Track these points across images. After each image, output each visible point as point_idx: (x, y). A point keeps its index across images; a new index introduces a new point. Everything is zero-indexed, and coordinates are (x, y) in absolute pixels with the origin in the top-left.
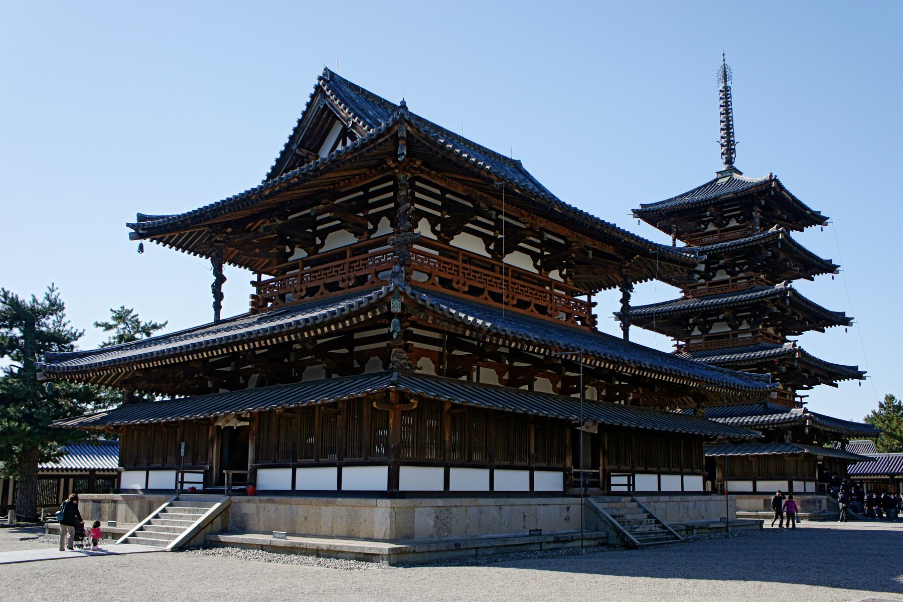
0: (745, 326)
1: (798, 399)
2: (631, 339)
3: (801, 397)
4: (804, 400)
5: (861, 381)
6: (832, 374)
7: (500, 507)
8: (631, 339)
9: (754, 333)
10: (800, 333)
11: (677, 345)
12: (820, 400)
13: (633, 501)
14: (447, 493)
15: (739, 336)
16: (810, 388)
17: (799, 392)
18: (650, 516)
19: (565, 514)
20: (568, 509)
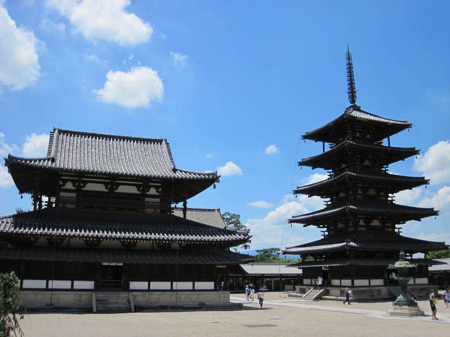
0: (351, 193)
1: (396, 230)
2: (187, 218)
3: (399, 229)
4: (400, 230)
5: (436, 216)
6: (418, 214)
7: (36, 295)
8: (187, 218)
10: (397, 191)
11: (327, 205)
12: (409, 229)
13: (128, 294)
15: (350, 198)
16: (404, 223)
17: (397, 226)
18: (129, 301)
19: (78, 298)
20: (80, 296)
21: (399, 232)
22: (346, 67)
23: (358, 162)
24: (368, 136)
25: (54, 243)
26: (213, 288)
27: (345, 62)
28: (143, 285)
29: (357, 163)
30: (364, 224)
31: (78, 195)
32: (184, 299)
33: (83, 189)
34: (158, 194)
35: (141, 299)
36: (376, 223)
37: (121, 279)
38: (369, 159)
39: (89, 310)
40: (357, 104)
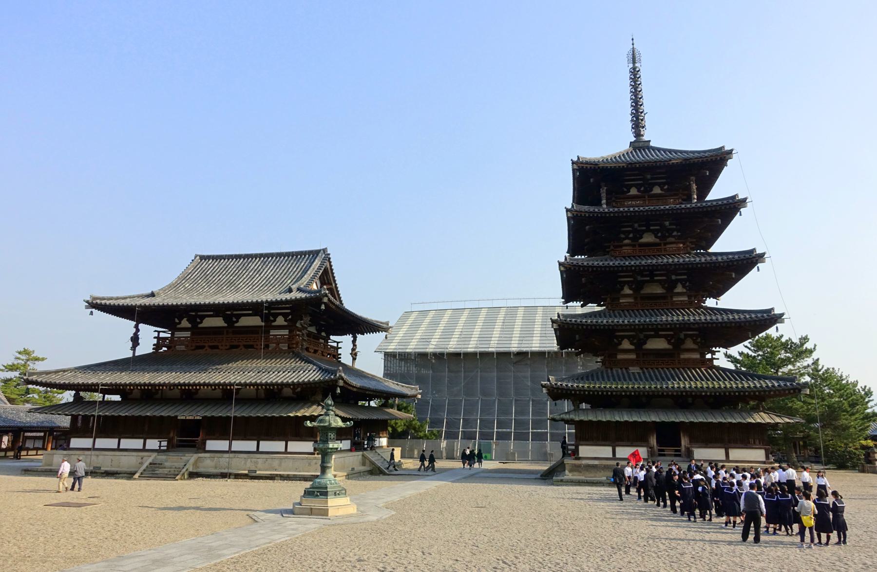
9: (636, 298)
14: (118, 449)
21: (713, 359)
22: (628, 75)
23: (629, 239)
24: (657, 190)
25: (189, 395)
26: (312, 450)
27: (627, 67)
28: (223, 445)
29: (627, 241)
30: (632, 347)
31: (192, 334)
32: (241, 465)
33: (236, 325)
34: (286, 323)
35: (208, 463)
36: (659, 344)
37: (198, 436)
38: (653, 231)
39: (130, 475)
40: (645, 138)
